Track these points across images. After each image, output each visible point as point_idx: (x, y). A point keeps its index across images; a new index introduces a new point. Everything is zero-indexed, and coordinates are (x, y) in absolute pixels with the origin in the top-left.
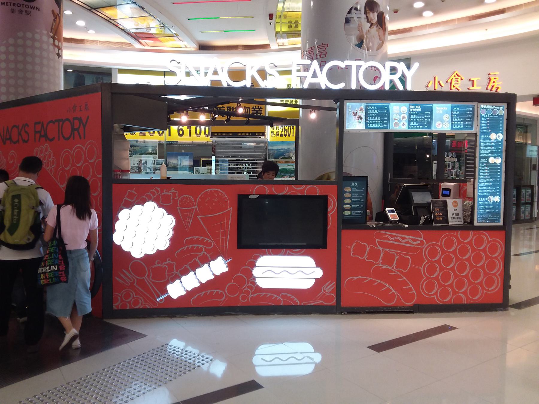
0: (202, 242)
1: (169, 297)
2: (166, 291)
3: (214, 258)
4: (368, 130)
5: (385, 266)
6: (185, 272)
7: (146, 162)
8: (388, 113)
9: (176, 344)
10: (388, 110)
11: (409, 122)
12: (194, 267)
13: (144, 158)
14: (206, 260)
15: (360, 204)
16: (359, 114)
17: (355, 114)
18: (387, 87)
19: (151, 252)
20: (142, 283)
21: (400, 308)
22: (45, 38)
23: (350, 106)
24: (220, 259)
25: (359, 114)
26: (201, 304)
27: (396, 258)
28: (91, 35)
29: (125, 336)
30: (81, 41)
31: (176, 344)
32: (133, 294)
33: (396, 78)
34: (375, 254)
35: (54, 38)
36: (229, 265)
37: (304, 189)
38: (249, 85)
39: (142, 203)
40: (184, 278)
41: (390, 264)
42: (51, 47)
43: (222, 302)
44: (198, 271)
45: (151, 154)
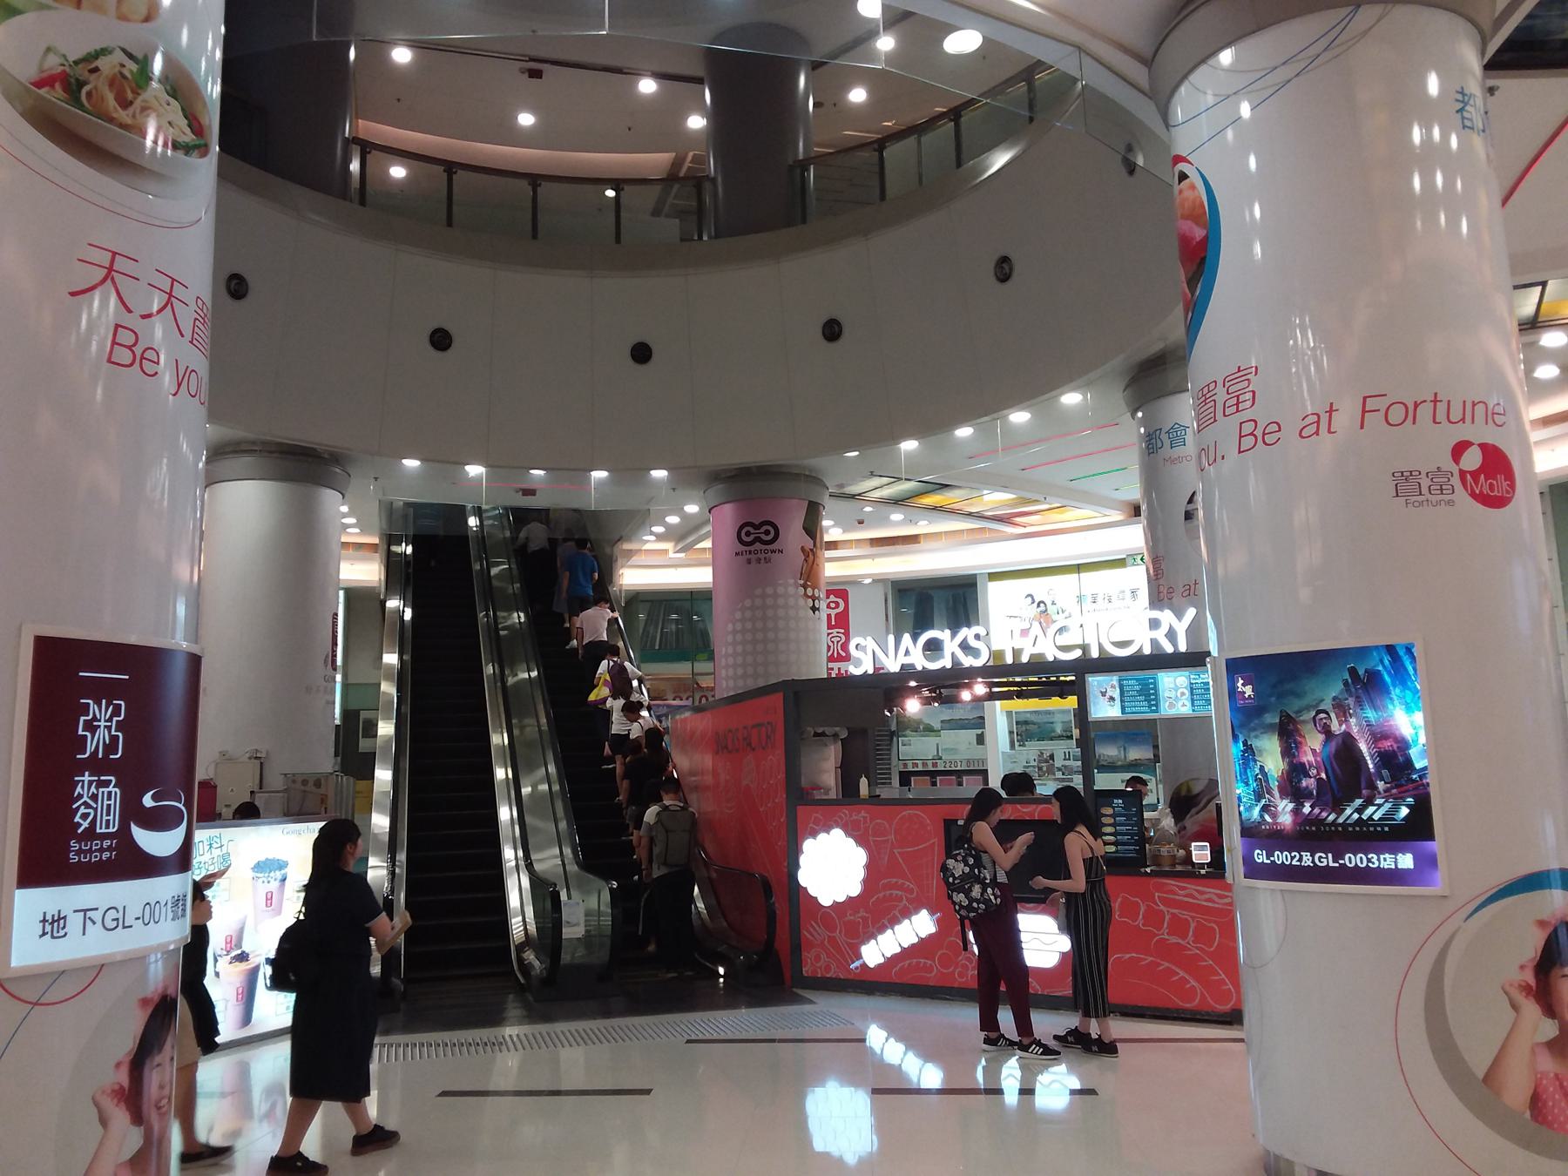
0: (901, 888)
1: (864, 965)
2: (859, 956)
3: (917, 911)
4: (1126, 717)
5: (1174, 939)
6: (882, 930)
7: (1052, 757)
8: (1156, 689)
9: (876, 1036)
10: (1155, 684)
11: (1193, 701)
12: (894, 922)
13: (1048, 746)
14: (907, 913)
15: (1132, 835)
16: (1109, 693)
17: (1104, 694)
18: (1147, 651)
19: (841, 899)
20: (832, 940)
21: (1208, 1014)
22: (791, 590)
23: (1094, 682)
24: (924, 913)
25: (1109, 693)
26: (907, 979)
27: (1193, 925)
28: (922, 527)
29: (797, 1000)
30: (913, 539)
31: (876, 1036)
32: (823, 956)
33: (1160, 636)
34: (1154, 918)
35: (805, 587)
36: (939, 922)
37: (1032, 814)
38: (949, 666)
39: (827, 830)
40: (880, 938)
41: (1184, 937)
42: (802, 602)
43: (932, 978)
44: (897, 928)
45: (1060, 737)
